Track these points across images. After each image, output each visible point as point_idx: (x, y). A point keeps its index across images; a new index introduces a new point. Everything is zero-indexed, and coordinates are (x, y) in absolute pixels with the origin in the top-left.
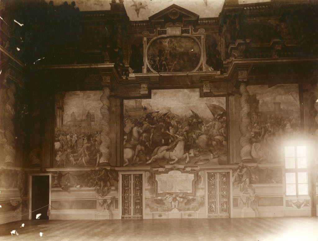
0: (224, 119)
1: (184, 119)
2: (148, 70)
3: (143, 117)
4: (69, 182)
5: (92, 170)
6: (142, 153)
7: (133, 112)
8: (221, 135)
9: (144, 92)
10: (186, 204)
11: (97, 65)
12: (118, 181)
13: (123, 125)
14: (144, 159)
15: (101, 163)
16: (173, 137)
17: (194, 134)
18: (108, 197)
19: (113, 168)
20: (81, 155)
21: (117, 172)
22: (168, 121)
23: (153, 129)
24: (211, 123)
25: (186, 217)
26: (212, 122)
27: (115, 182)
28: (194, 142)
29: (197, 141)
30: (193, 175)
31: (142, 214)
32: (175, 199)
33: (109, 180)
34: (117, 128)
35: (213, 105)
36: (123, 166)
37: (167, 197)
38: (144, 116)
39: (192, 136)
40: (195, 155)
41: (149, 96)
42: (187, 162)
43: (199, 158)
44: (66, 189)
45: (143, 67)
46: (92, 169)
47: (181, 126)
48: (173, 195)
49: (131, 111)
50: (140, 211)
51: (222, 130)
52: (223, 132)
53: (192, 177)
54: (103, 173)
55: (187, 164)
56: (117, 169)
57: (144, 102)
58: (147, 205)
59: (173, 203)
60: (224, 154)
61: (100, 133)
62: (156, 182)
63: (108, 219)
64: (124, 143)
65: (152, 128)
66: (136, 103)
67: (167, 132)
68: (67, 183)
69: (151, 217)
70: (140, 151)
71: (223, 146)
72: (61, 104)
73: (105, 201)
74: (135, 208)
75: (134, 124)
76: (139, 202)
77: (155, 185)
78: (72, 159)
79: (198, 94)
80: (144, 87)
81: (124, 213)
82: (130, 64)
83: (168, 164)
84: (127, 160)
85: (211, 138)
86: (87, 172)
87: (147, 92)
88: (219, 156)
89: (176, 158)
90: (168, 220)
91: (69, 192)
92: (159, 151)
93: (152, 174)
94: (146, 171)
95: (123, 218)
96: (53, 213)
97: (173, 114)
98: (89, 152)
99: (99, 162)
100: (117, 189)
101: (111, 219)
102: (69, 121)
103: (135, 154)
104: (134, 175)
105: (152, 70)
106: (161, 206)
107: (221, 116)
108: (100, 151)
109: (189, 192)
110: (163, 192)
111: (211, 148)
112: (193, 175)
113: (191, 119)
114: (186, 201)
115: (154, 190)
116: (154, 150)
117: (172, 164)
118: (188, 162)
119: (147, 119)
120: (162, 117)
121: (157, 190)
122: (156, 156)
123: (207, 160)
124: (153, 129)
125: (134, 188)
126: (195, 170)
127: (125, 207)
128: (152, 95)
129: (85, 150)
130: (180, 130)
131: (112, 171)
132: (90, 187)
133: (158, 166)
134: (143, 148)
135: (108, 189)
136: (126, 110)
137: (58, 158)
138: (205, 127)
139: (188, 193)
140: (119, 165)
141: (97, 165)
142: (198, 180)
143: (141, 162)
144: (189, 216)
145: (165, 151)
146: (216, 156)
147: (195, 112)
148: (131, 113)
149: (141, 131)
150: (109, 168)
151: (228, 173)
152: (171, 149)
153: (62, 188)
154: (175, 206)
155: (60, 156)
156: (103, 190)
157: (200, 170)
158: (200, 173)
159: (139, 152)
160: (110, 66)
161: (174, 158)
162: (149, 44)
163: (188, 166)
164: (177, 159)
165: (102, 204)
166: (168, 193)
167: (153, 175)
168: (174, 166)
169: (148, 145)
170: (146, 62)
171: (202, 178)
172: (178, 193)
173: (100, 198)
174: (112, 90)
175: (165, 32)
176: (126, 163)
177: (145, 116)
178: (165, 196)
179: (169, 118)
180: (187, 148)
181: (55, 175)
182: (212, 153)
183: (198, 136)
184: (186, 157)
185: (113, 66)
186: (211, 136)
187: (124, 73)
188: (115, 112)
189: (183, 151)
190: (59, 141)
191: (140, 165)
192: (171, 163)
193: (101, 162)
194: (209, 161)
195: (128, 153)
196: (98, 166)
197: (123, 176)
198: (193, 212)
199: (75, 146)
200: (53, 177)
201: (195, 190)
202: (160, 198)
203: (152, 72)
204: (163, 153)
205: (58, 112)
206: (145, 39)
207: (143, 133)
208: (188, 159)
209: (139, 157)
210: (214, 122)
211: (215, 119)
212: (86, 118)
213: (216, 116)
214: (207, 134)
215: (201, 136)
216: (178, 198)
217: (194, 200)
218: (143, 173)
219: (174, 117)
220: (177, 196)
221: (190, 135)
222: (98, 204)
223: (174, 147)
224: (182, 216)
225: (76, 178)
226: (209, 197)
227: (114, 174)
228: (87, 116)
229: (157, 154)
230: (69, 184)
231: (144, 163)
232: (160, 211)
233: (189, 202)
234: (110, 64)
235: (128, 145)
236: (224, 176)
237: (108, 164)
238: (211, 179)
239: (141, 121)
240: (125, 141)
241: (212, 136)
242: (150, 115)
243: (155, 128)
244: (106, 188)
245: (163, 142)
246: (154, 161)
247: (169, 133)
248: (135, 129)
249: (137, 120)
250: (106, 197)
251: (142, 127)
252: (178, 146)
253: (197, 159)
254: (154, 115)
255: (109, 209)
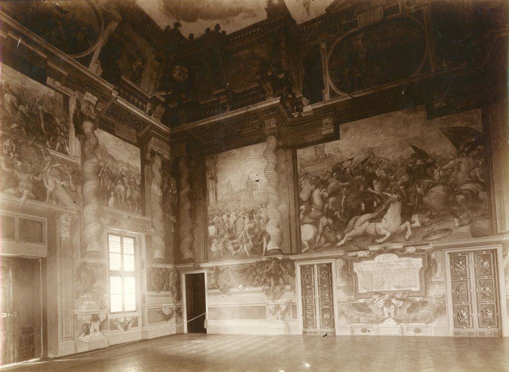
0: (479, 149)
1: (399, 163)
2: (333, 94)
3: (328, 172)
4: (229, 281)
5: (257, 262)
6: (329, 230)
7: (311, 165)
8: (475, 180)
9: (327, 131)
10: (410, 311)
11: (257, 106)
12: (294, 276)
13: (297, 189)
14: (332, 239)
15: (269, 251)
16: (379, 197)
17: (419, 187)
18: (282, 301)
19: (286, 257)
20: (241, 241)
21: (292, 262)
22: (371, 170)
23: (345, 189)
24: (451, 163)
25: (412, 333)
26: (452, 160)
27: (291, 279)
28: (421, 202)
29: (425, 199)
30: (420, 260)
31: (334, 327)
32: (388, 303)
33: (281, 276)
34: (289, 195)
35: (455, 127)
36: (301, 253)
37: (375, 300)
38: (330, 169)
39: (416, 191)
40: (423, 225)
41: (335, 136)
42: (407, 237)
43: (430, 229)
44: (225, 290)
45: (323, 91)
46: (258, 261)
47: (393, 177)
48: (384, 295)
49: (308, 166)
50: (331, 323)
51: (477, 172)
52: (478, 175)
53: (418, 262)
54: (272, 265)
55: (408, 240)
56: (292, 257)
57: (329, 148)
58: (342, 313)
59: (385, 309)
60: (482, 216)
61: (266, 206)
62: (355, 274)
63: (284, 334)
64: (301, 216)
65: (344, 186)
66: (316, 151)
67: (370, 189)
68: (226, 282)
69: (349, 333)
70: (325, 226)
71: (481, 201)
72: (213, 172)
73: (278, 307)
74: (323, 317)
75: (314, 184)
76: (328, 309)
77: (352, 280)
78: (231, 248)
79: (423, 114)
80: (327, 124)
81: (306, 325)
82: (303, 93)
83: (373, 243)
84: (306, 243)
85: (453, 190)
86: (251, 265)
87: (332, 130)
88: (471, 222)
89: (386, 231)
90: (378, 337)
91: (229, 295)
92: (357, 224)
93: (347, 262)
94: (336, 258)
95: (305, 333)
96: (210, 324)
97: (379, 158)
98: (253, 236)
99: (266, 249)
100: (293, 288)
101: (287, 334)
102: (224, 195)
103: (318, 232)
104: (318, 265)
105: (338, 93)
106: (364, 315)
107: (473, 146)
108: (267, 233)
109: (414, 289)
110: (367, 291)
111: (454, 208)
112: (420, 260)
113: (412, 161)
114: (409, 305)
115: (352, 289)
116: (348, 223)
117: (380, 243)
118: (410, 238)
119: (334, 174)
120: (360, 166)
121: (356, 287)
122: (352, 233)
123: (447, 230)
124: (345, 189)
125: (319, 286)
126: (423, 251)
127: (308, 317)
128: (341, 132)
129: (247, 233)
130: (392, 183)
131: (284, 262)
132: (256, 286)
133: (357, 248)
134: (330, 221)
135: (281, 289)
136: (301, 165)
137: (213, 248)
138: (441, 172)
139: (412, 292)
140: (294, 251)
141: (264, 254)
142: (429, 267)
143: (328, 244)
144: (415, 332)
145: (367, 223)
146: (466, 222)
147: (419, 147)
148: (310, 169)
149: (326, 195)
150: (280, 257)
151: (493, 252)
152: (377, 218)
153: (221, 290)
154: (389, 314)
155: (216, 246)
156: (274, 291)
157: (435, 249)
158: (433, 255)
159: (324, 228)
160: (275, 102)
161: (383, 233)
162: (330, 52)
163: (408, 245)
164: (388, 235)
165: (273, 311)
166: (376, 293)
167: (349, 264)
168: (383, 246)
169: (339, 216)
170: (328, 81)
171: (439, 265)
172: (393, 291)
173: (270, 302)
174: (279, 138)
175: (355, 24)
176: (305, 247)
177: (331, 169)
178: (370, 298)
179: (371, 165)
180: (406, 215)
181: (212, 272)
182: (457, 217)
183: (427, 190)
184: (406, 227)
185: (279, 101)
186: (453, 186)
187: (295, 108)
188: (284, 171)
189: (399, 219)
190: (213, 224)
191: (327, 249)
192: (378, 241)
193: (269, 249)
194: (452, 231)
195: (308, 232)
196: (265, 255)
197: (302, 267)
198: (424, 324)
199: (234, 230)
200: (209, 275)
201: (426, 287)
202: (361, 301)
203: (339, 96)
204: (364, 227)
205: (210, 184)
206: (323, 46)
207: (330, 196)
208: (409, 232)
209: (324, 236)
210: (458, 160)
211: (459, 154)
212: (246, 187)
213: (461, 148)
214: (444, 184)
215: (432, 189)
216: (394, 301)
217: (424, 303)
218: (333, 261)
219: (381, 163)
220: (392, 297)
221: (411, 189)
222: (268, 312)
223: (384, 215)
224: (402, 332)
225: (237, 274)
226: (456, 298)
227: (289, 266)
228: (247, 183)
229: (353, 228)
230: (228, 284)
231: (333, 245)
232: (363, 323)
233: (414, 307)
234: (275, 99)
235: (307, 220)
236: (486, 257)
237: (280, 251)
238: (458, 265)
239: (325, 179)
240: (302, 213)
241: (456, 185)
242: (338, 167)
243: (348, 187)
244: (278, 288)
245: (363, 208)
246: (348, 241)
247: (374, 191)
248: (317, 193)
249: (318, 178)
250: (278, 302)
251: (327, 187)
252: (389, 211)
253: (426, 230)
254: (346, 165)
255: (283, 319)
